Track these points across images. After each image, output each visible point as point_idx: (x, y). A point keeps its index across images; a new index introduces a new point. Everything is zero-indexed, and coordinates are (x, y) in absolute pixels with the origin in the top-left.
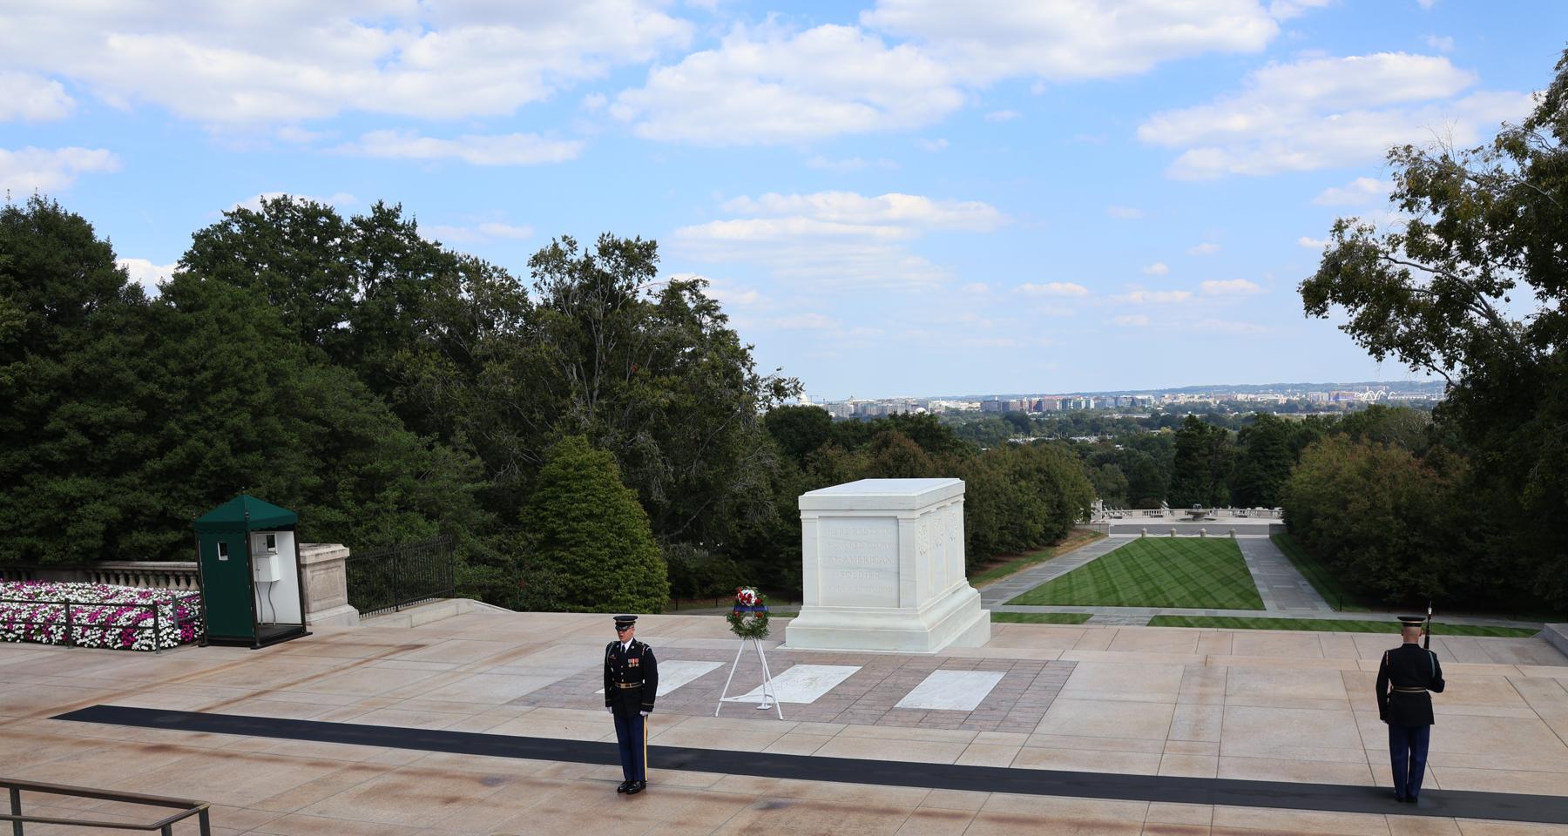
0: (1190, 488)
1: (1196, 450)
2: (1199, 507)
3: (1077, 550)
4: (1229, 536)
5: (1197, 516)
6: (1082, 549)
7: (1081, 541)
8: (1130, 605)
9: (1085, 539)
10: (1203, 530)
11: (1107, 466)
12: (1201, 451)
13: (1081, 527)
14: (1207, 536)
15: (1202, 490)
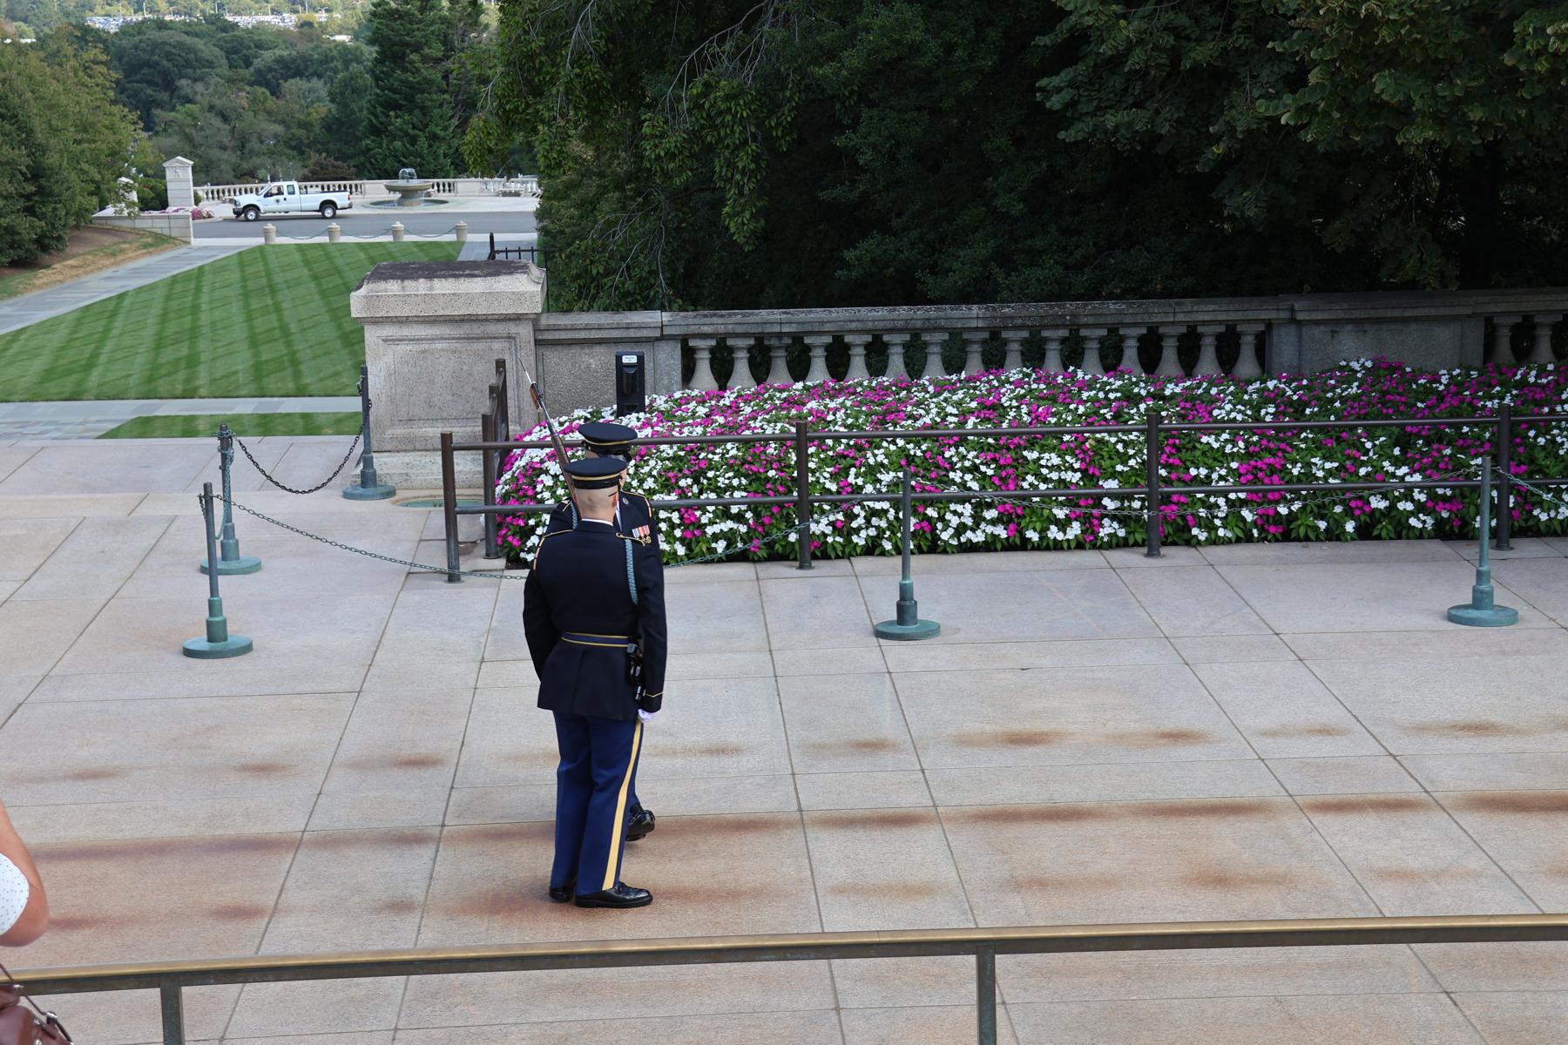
0: (407, 134)
1: (417, 48)
2: (411, 176)
3: (83, 279)
4: (452, 237)
5: (408, 195)
6: (108, 273)
7: (113, 254)
8: (97, 398)
9: (122, 251)
10: (398, 225)
11: (293, 85)
12: (427, 51)
13: (126, 224)
14: (408, 238)
15: (434, 138)
